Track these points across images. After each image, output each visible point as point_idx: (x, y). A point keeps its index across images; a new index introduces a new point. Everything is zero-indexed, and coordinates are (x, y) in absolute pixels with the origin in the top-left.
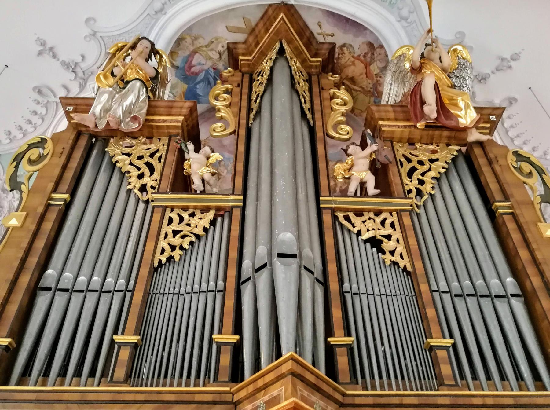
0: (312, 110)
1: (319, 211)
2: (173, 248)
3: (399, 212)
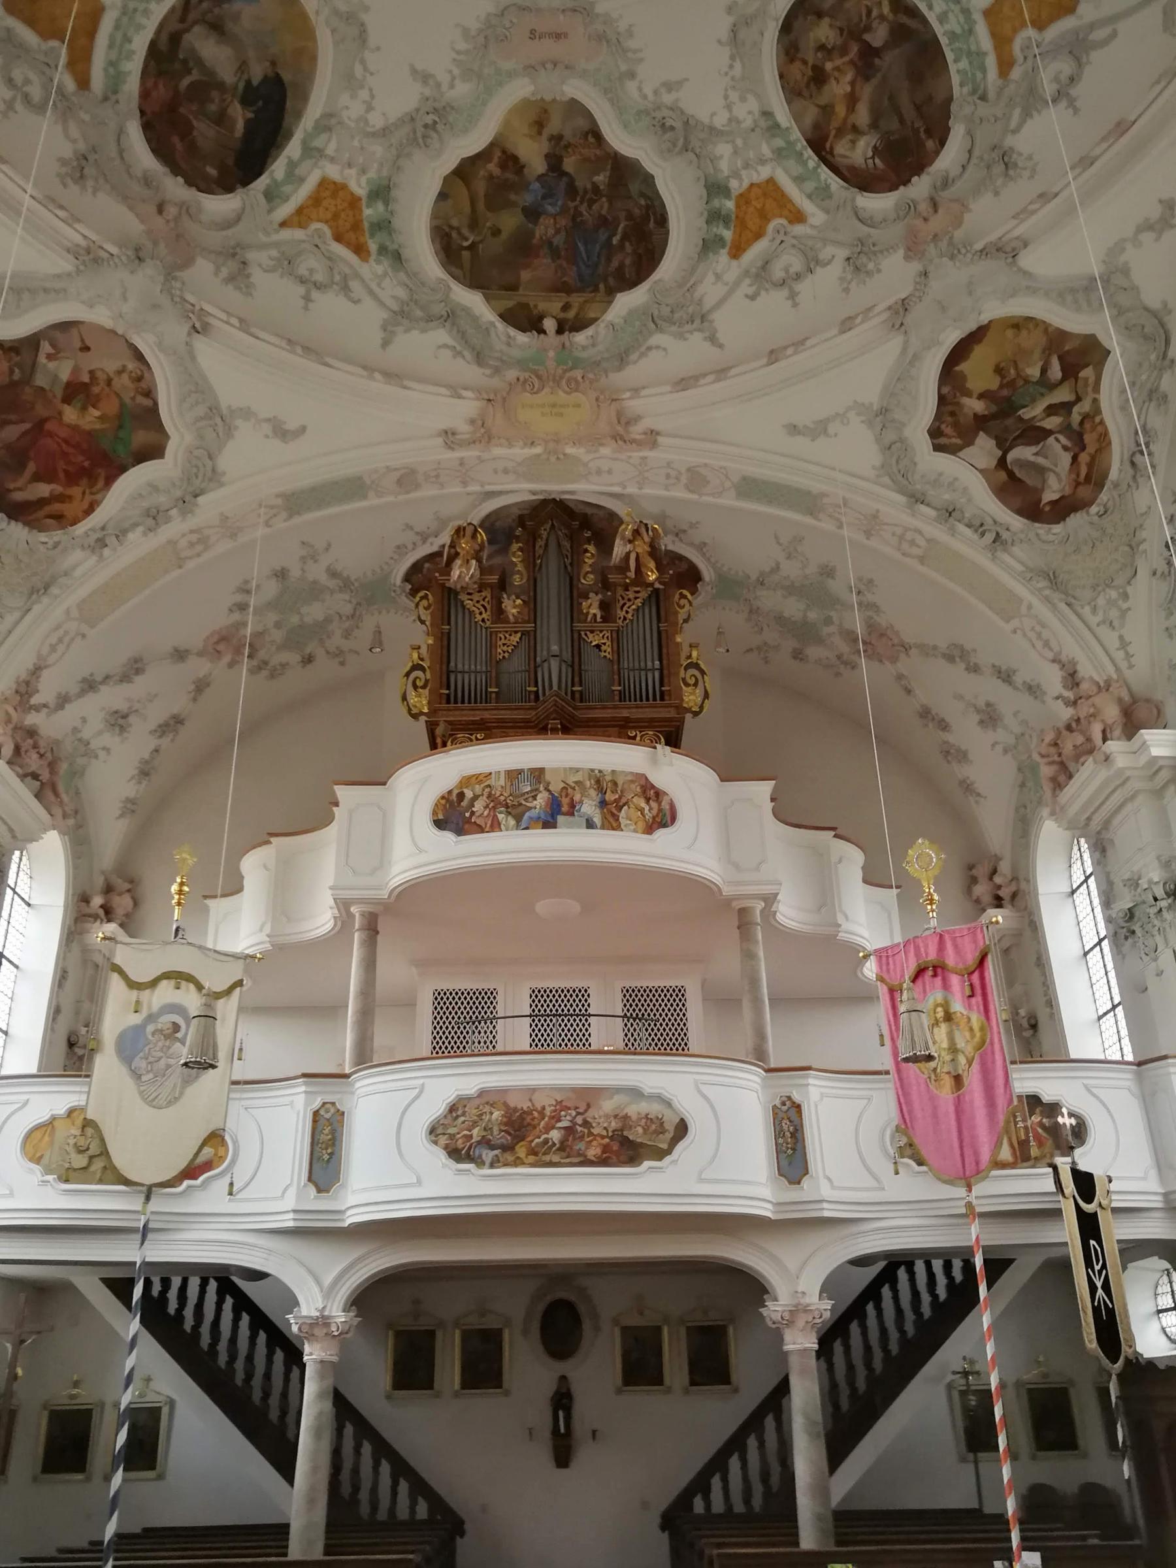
0: (571, 564)
1: (572, 631)
2: (504, 652)
3: (612, 631)
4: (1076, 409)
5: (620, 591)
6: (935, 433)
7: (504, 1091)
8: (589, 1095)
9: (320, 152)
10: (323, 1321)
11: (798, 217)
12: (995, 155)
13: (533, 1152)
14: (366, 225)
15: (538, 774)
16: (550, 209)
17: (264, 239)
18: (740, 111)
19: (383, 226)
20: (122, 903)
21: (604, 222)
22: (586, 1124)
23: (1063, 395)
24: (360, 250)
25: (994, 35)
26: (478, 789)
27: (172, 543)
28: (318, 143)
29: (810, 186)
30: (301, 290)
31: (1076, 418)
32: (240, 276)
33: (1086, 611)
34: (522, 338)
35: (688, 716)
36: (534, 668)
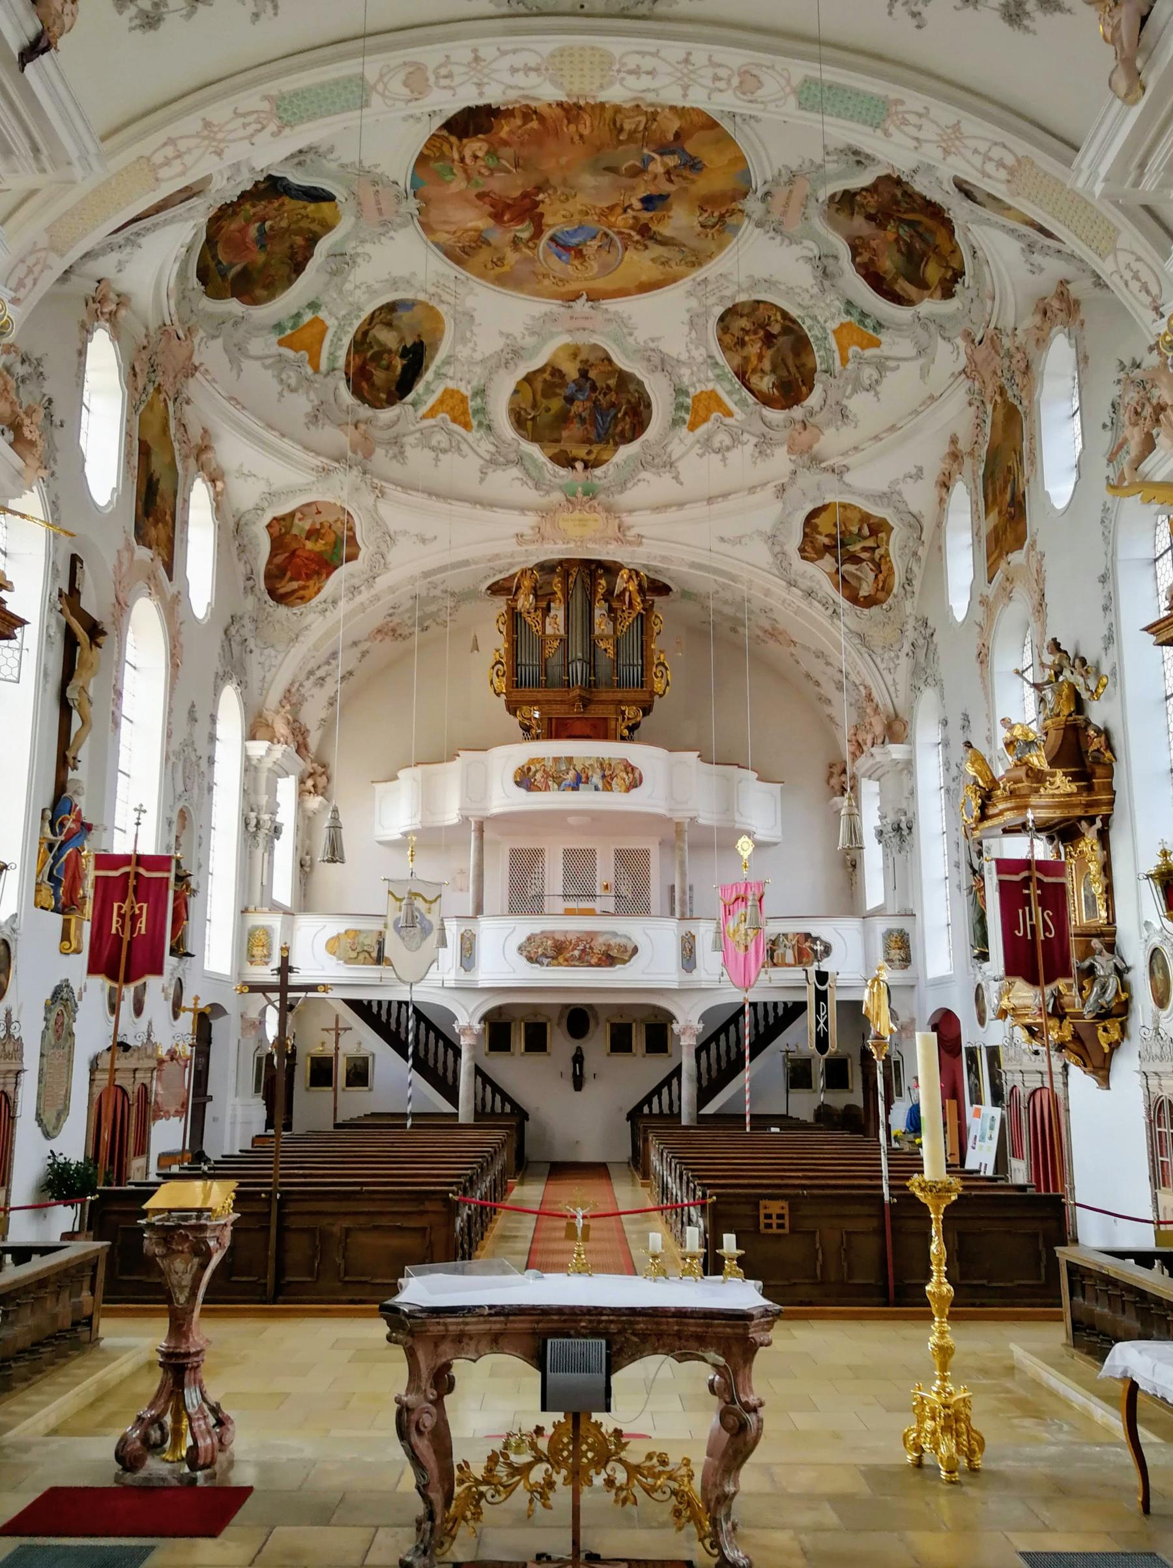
4: (877, 551)
5: (619, 613)
6: (802, 550)
7: (553, 932)
8: (592, 935)
9: (445, 375)
10: (470, 1028)
11: (730, 414)
12: (838, 408)
13: (566, 960)
14: (470, 411)
15: (570, 760)
16: (581, 397)
17: (412, 428)
18: (695, 353)
19: (481, 411)
20: (322, 781)
21: (613, 405)
22: (591, 948)
23: (870, 543)
24: (467, 426)
25: (838, 343)
26: (538, 766)
27: (362, 604)
28: (443, 371)
29: (736, 397)
30: (433, 455)
31: (877, 556)
32: (400, 456)
33: (878, 661)
34: (563, 472)
35: (656, 698)
36: (567, 664)
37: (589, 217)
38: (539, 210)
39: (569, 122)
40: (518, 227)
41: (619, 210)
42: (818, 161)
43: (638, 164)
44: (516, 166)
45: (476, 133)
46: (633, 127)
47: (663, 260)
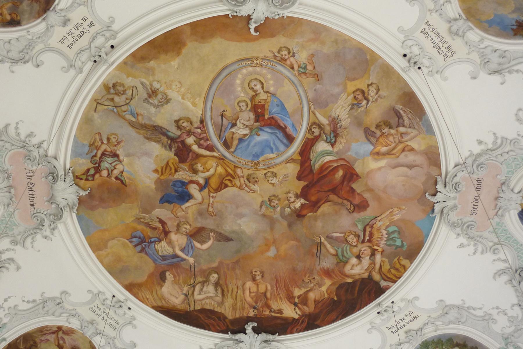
37: (246, 172)
38: (303, 184)
39: (265, 294)
40: (328, 158)
41: (214, 182)
42: (18, 248)
43: (198, 245)
44: (320, 245)
45: (354, 283)
46: (205, 289)
47: (156, 102)
